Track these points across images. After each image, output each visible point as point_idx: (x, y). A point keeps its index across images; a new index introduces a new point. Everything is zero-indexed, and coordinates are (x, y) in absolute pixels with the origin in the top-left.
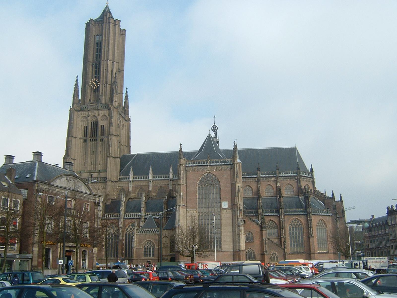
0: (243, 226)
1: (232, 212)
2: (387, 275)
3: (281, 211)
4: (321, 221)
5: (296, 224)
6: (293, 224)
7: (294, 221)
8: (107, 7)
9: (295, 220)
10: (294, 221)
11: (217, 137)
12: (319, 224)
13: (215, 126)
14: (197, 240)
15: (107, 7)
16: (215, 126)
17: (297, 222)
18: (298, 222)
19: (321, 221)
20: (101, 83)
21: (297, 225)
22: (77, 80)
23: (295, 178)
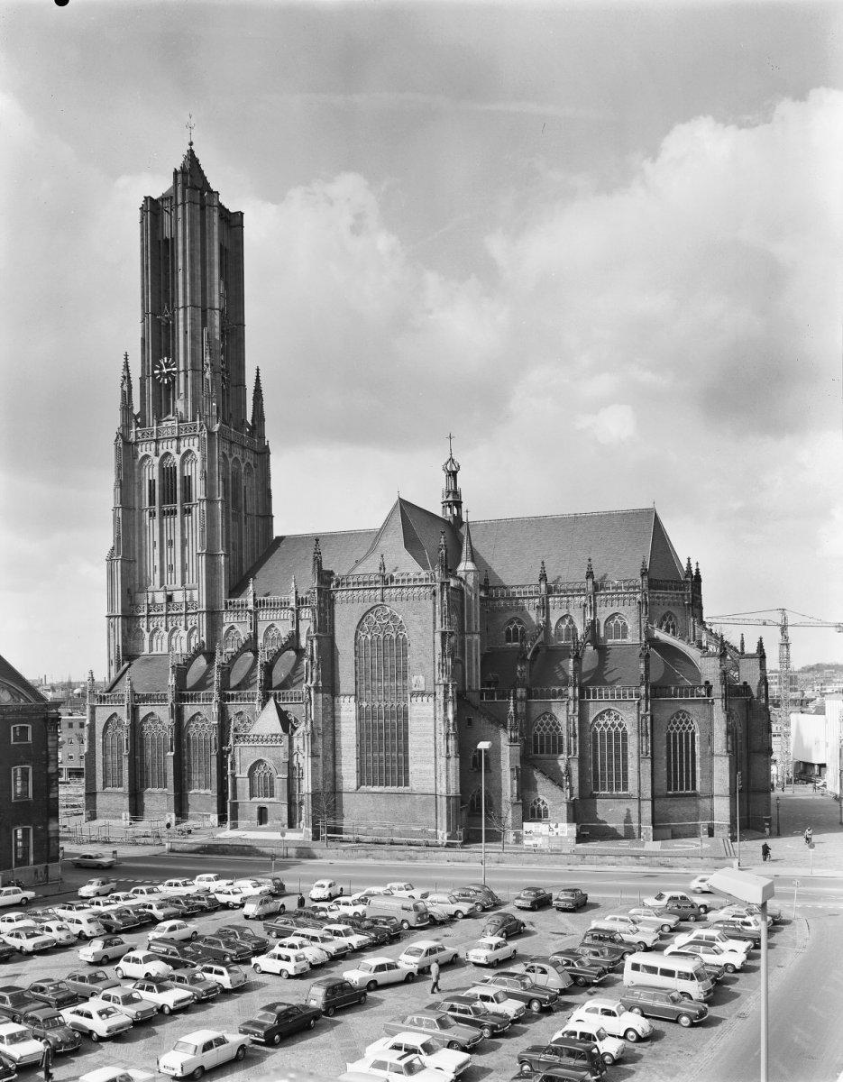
0: (455, 738)
1: (435, 700)
2: (597, 892)
3: (574, 692)
4: (681, 715)
5: (609, 723)
6: (602, 722)
7: (607, 717)
8: (192, 158)
9: (609, 715)
10: (607, 717)
12: (675, 723)
14: (577, 713)
15: (192, 158)
16: (452, 460)
17: (613, 718)
18: (617, 718)
19: (681, 715)
20: (181, 368)
21: (613, 725)
22: (126, 367)
23: (635, 598)
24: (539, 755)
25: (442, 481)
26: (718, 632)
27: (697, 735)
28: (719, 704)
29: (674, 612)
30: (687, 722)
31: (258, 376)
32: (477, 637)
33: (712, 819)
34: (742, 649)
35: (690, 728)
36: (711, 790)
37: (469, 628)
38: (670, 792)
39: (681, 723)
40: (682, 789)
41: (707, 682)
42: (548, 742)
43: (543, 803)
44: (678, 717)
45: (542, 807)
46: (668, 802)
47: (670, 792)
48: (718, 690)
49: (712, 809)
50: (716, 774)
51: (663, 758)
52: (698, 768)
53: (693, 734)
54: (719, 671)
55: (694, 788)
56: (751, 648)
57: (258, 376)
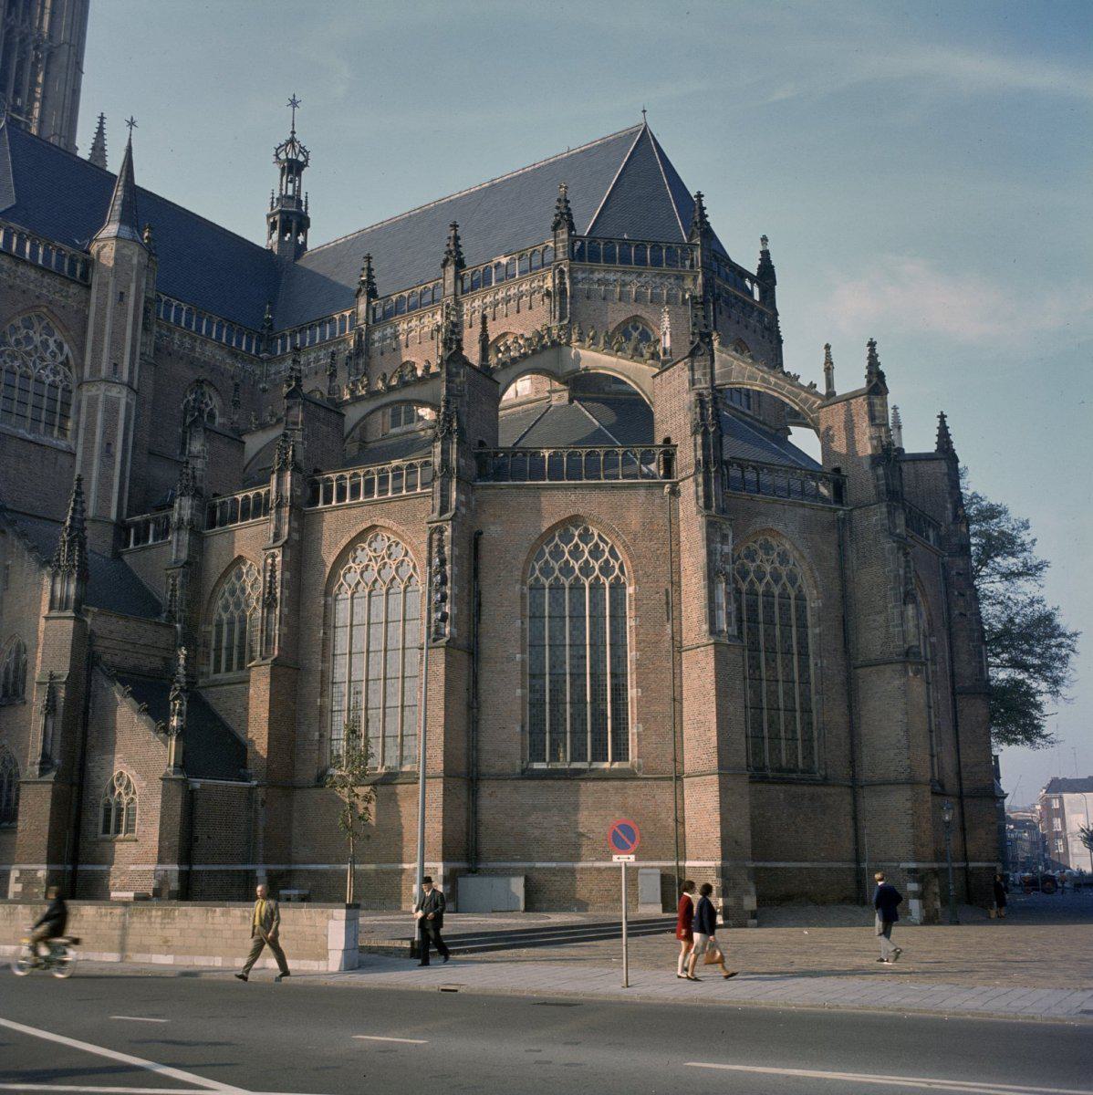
11: (303, 198)
12: (557, 554)
13: (292, 141)
24: (223, 676)
25: (271, 182)
26: (1043, 574)
27: (630, 590)
28: (690, 490)
29: (645, 315)
30: (596, 553)
31: (130, 139)
32: (121, 395)
33: (681, 854)
34: (829, 383)
35: (606, 570)
36: (677, 759)
37: (96, 368)
38: (538, 766)
39: (576, 553)
40: (578, 755)
41: (667, 440)
42: (231, 631)
43: (128, 786)
44: (567, 538)
45: (125, 800)
46: (527, 794)
47: (538, 766)
48: (688, 455)
49: (680, 821)
50: (689, 708)
51: (510, 659)
52: (632, 693)
53: (618, 587)
54: (692, 397)
55: (620, 754)
56: (851, 379)
57: (130, 139)
